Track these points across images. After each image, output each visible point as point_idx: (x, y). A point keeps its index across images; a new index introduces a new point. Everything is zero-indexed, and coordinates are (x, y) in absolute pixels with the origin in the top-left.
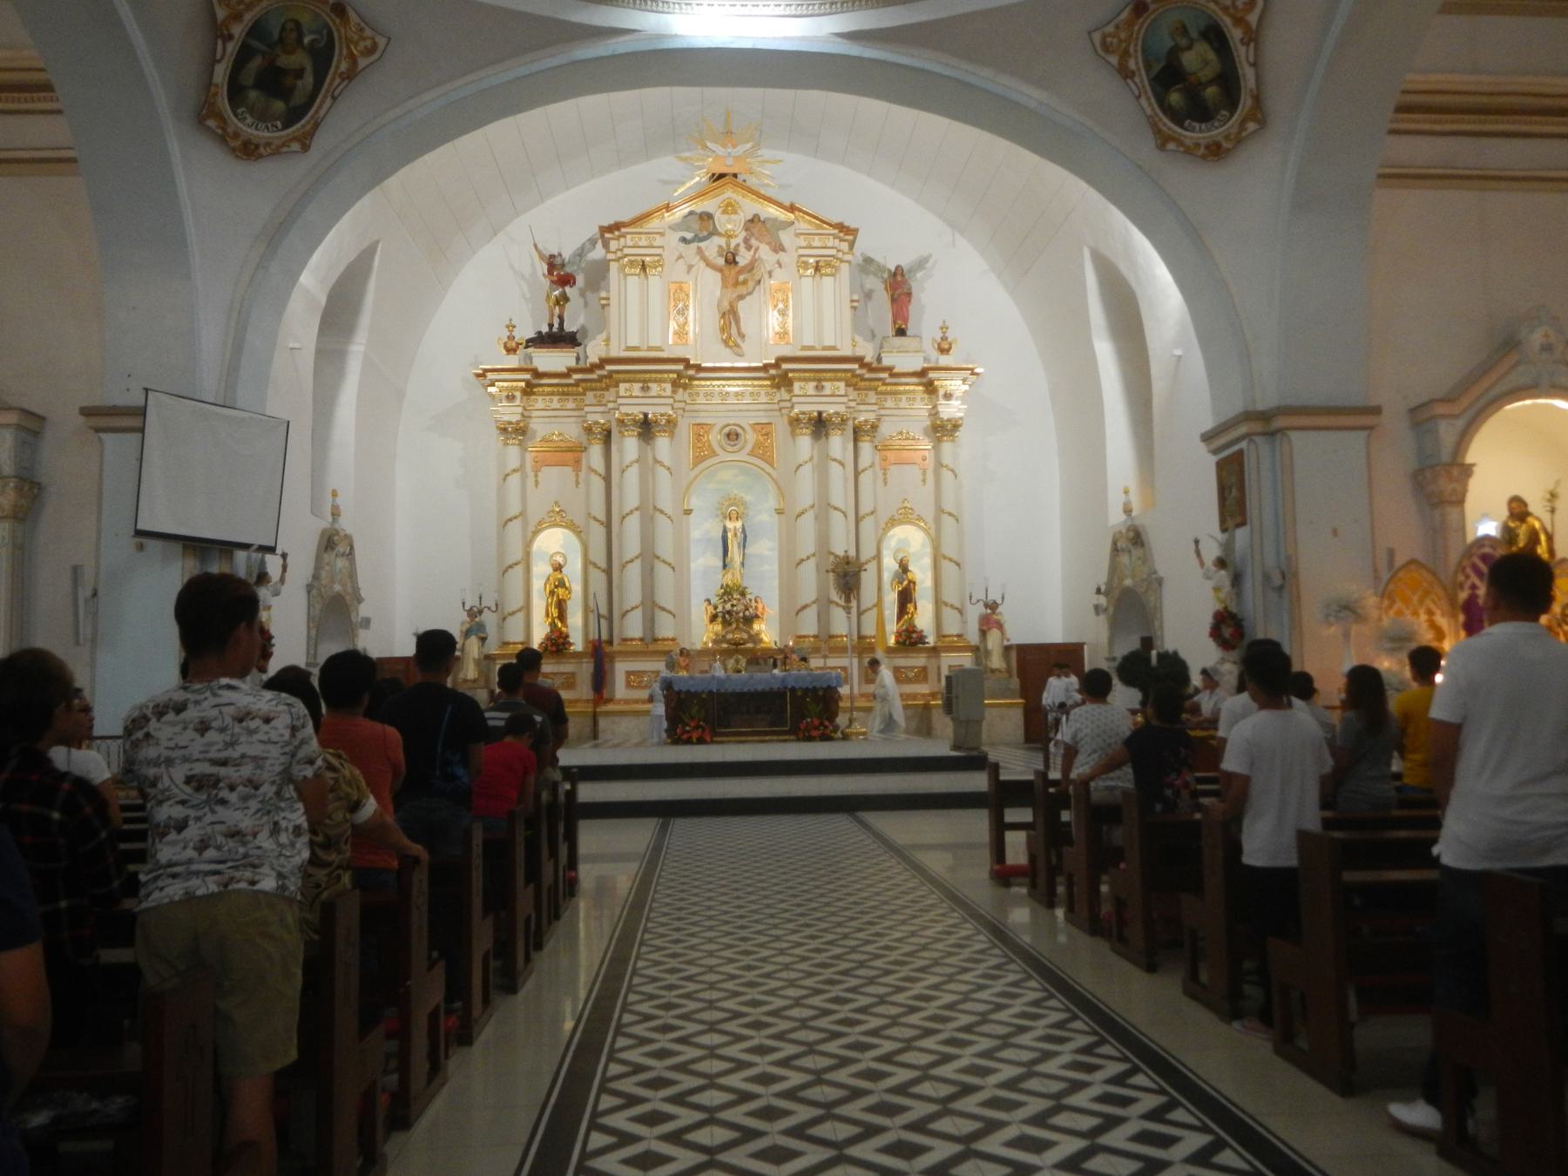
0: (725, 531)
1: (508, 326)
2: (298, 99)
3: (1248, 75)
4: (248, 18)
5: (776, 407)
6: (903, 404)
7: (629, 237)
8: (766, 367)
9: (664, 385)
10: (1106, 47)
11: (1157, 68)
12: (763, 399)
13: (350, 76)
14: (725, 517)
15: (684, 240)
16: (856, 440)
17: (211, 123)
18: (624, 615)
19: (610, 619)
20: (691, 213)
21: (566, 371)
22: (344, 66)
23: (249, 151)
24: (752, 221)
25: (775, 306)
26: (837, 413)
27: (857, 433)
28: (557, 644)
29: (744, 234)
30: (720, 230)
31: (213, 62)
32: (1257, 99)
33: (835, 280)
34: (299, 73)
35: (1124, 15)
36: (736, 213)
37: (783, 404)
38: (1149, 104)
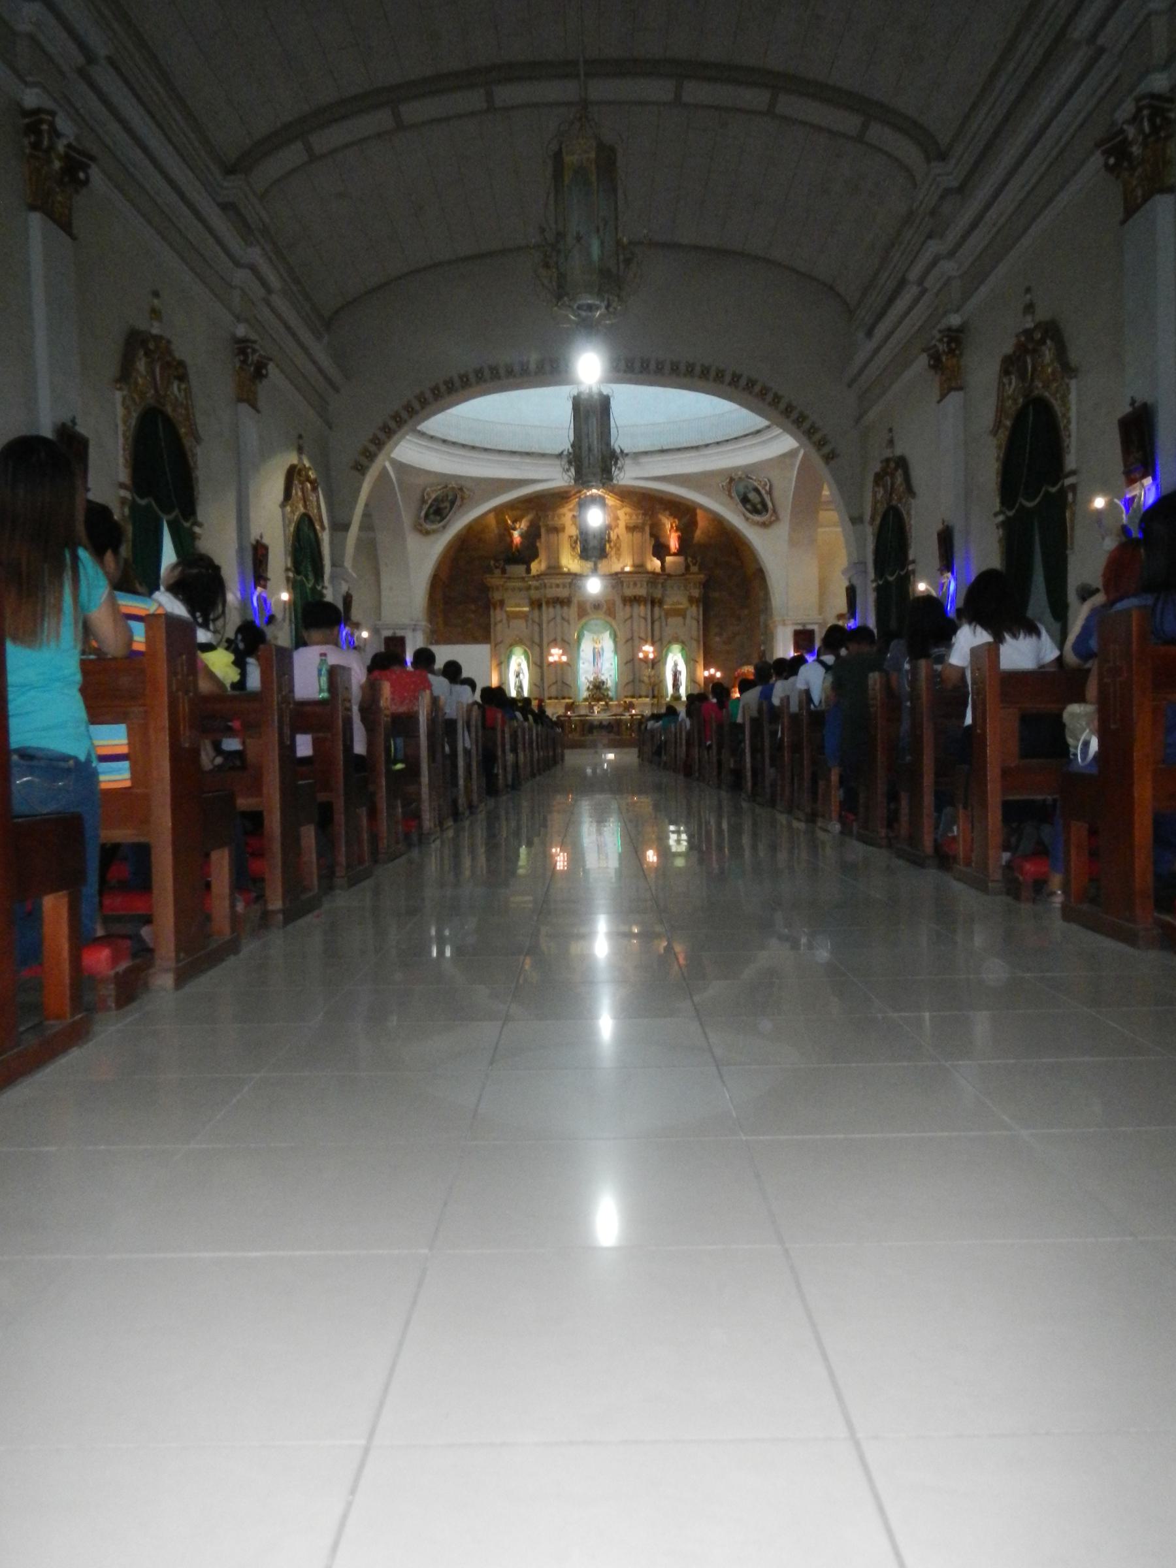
0: (594, 649)
2: (444, 515)
3: (770, 505)
4: (433, 496)
10: (724, 489)
11: (741, 497)
13: (461, 506)
17: (419, 528)
18: (549, 687)
22: (459, 504)
23: (427, 533)
27: (653, 603)
31: (421, 509)
32: (774, 511)
33: (642, 536)
35: (728, 480)
38: (740, 506)
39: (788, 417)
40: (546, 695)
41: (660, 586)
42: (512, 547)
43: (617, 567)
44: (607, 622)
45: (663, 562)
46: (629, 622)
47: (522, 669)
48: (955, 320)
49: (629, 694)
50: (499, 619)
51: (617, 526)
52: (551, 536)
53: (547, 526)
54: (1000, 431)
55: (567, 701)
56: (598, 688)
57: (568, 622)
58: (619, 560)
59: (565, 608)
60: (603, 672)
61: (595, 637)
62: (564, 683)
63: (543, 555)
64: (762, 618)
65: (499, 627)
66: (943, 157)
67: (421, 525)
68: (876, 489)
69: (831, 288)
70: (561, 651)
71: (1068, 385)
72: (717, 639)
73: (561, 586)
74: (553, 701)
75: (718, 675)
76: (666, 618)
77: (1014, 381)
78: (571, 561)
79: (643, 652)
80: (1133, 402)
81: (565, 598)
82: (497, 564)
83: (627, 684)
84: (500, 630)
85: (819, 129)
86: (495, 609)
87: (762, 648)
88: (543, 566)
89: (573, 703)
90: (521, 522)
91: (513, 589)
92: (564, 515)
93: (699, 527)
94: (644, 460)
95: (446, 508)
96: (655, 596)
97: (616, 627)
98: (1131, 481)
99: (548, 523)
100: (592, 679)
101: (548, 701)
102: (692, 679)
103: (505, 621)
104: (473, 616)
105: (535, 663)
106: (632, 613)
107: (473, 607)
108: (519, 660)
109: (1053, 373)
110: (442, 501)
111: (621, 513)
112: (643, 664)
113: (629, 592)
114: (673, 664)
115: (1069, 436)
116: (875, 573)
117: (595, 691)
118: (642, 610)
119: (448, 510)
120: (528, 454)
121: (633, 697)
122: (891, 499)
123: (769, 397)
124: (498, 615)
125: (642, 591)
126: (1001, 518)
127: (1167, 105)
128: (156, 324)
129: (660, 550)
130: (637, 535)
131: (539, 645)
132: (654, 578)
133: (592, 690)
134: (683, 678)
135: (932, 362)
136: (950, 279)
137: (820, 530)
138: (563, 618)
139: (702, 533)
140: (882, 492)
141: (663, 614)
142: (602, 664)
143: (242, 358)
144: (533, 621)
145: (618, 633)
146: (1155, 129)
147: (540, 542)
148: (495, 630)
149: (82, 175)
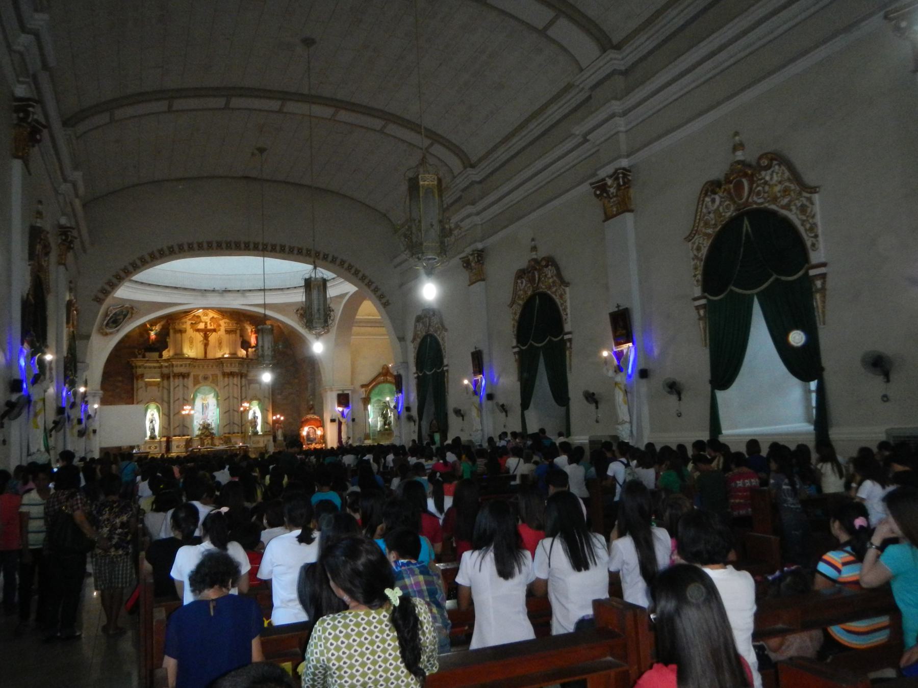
0: (203, 404)
4: (114, 312)
8: (216, 359)
13: (129, 318)
15: (192, 323)
16: (241, 378)
17: (101, 331)
23: (106, 334)
28: (153, 437)
30: (203, 320)
34: (120, 319)
39: (363, 282)
40: (172, 434)
41: (246, 366)
42: (149, 342)
43: (219, 355)
44: (213, 388)
45: (247, 351)
46: (227, 387)
48: (480, 246)
49: (227, 432)
51: (219, 330)
53: (175, 328)
54: (514, 306)
55: (187, 437)
56: (206, 427)
57: (188, 388)
59: (186, 379)
60: (208, 418)
61: (204, 397)
62: (184, 426)
63: (171, 345)
64: (310, 385)
65: (140, 392)
66: (473, 166)
67: (103, 329)
68: (417, 324)
69: (385, 215)
70: (190, 407)
71: (564, 290)
72: (279, 397)
75: (282, 418)
76: (249, 386)
77: (524, 282)
78: (189, 351)
79: (244, 407)
80: (618, 306)
82: (140, 352)
84: (141, 394)
85: (403, 141)
86: (137, 380)
87: (311, 403)
88: (171, 353)
89: (191, 439)
91: (150, 368)
94: (248, 294)
95: (120, 319)
96: (242, 371)
97: (217, 389)
98: (618, 344)
99: (176, 327)
100: (201, 423)
102: (265, 421)
103: (144, 388)
104: (120, 384)
105: (164, 414)
107: (120, 378)
108: (152, 412)
109: (554, 282)
110: (119, 315)
111: (222, 322)
113: (228, 369)
115: (567, 314)
116: (417, 369)
117: (204, 430)
118: (236, 380)
119: (121, 320)
120: (176, 288)
121: (229, 433)
122: (429, 330)
123: (353, 271)
124: (141, 383)
125: (235, 369)
126: (516, 350)
127: (628, 173)
128: (39, 220)
129: (245, 345)
130: (233, 336)
131: (167, 403)
132: (243, 361)
133: (202, 430)
134: (259, 421)
135: (465, 265)
136: (476, 225)
137: (353, 337)
138: (184, 386)
140: (421, 325)
141: (247, 382)
143: (64, 238)
144: (163, 387)
145: (220, 395)
146: (625, 183)
148: (137, 393)
149: (38, 137)
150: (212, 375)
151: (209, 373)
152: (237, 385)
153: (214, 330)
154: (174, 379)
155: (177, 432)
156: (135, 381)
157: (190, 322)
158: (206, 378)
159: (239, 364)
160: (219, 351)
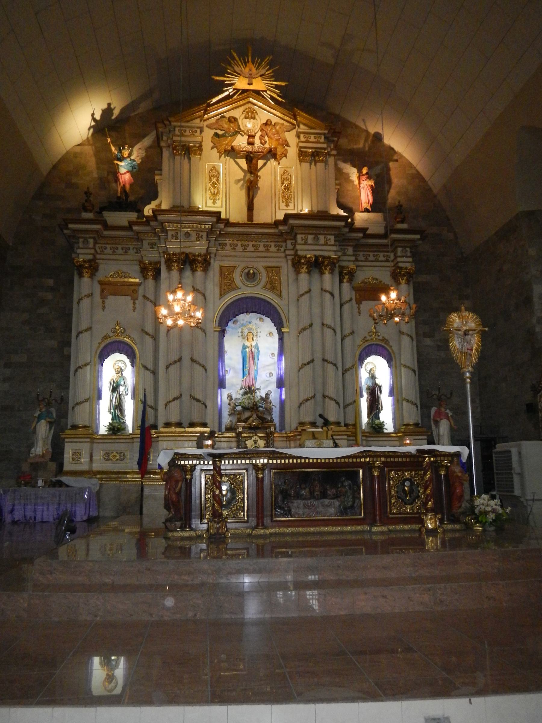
0: (244, 347)
1: (86, 193)
5: (283, 255)
6: (371, 258)
7: (177, 129)
8: (277, 223)
9: (201, 233)
12: (273, 249)
14: (244, 338)
15: (216, 135)
16: (341, 282)
19: (156, 410)
20: (223, 117)
21: (126, 224)
24: (266, 124)
25: (283, 183)
26: (329, 258)
29: (259, 133)
30: (242, 129)
36: (254, 118)
37: (288, 252)
40: (161, 422)
47: (124, 379)
50: (86, 291)
52: (177, 158)
57: (204, 295)
58: (287, 205)
59: (199, 273)
65: (85, 303)
72: (428, 341)
73: (194, 235)
74: (173, 429)
76: (359, 302)
81: (200, 255)
83: (307, 400)
86: (81, 275)
90: (131, 146)
92: (201, 131)
93: (393, 185)
99: (175, 138)
101: (162, 430)
104: (49, 296)
106: (310, 283)
107: (51, 282)
108: (122, 365)
111: (291, 137)
112: (330, 365)
114: (367, 375)
131: (152, 337)
133: (240, 413)
139: (399, 193)
142: (257, 371)
147: (161, 175)
150: (266, 268)
151: (260, 265)
152: (332, 295)
153: (272, 154)
154: (169, 268)
155: (174, 419)
156: (76, 278)
157: (213, 132)
158: (251, 276)
159: (336, 236)
160: (283, 205)
